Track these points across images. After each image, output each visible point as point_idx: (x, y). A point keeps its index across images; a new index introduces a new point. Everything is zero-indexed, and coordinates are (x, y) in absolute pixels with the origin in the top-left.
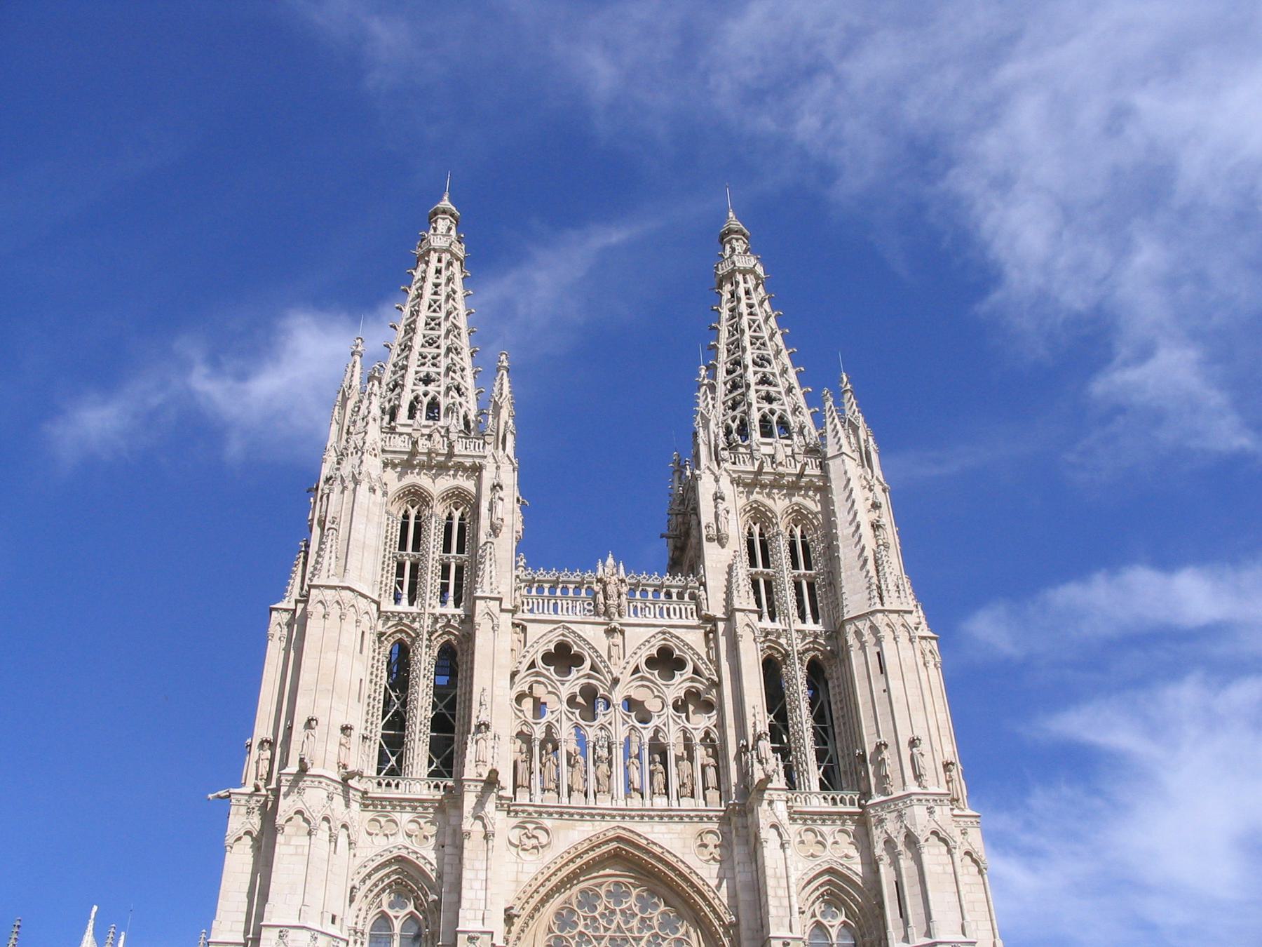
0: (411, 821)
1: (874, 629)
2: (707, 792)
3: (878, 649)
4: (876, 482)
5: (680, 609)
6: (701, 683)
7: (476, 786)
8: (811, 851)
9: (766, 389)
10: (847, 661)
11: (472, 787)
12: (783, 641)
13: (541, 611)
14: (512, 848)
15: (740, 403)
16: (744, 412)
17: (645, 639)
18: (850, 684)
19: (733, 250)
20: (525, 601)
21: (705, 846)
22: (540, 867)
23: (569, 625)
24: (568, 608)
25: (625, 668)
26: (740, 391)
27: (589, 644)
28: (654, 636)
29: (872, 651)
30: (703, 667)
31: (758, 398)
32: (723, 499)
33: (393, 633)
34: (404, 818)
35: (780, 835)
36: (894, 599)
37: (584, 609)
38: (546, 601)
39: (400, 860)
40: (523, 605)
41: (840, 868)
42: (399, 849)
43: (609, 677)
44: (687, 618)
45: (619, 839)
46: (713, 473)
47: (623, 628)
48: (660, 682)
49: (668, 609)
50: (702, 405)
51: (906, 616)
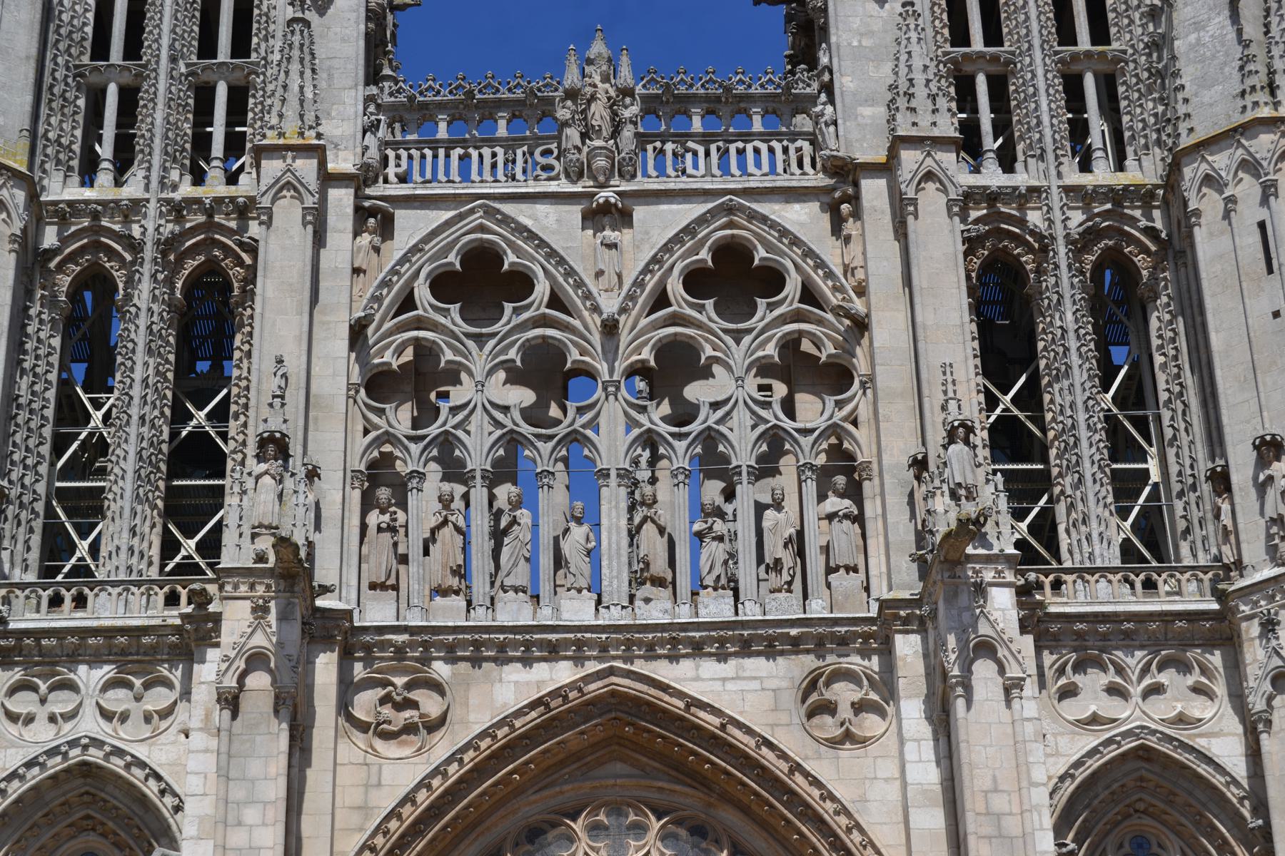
0: (110, 685)
1: (1250, 166)
2: (832, 577)
3: (1263, 214)
5: (771, 151)
6: (820, 322)
7: (252, 587)
8: (1093, 708)
10: (1189, 252)
11: (243, 589)
12: (1034, 218)
13: (428, 176)
14: (359, 737)
18: (1196, 310)
20: (391, 153)
21: (828, 708)
22: (420, 770)
24: (494, 166)
27: (542, 244)
28: (702, 220)
29: (1250, 212)
30: (825, 287)
33: (82, 250)
34: (90, 677)
35: (1002, 670)
38: (441, 152)
39: (86, 769)
40: (386, 166)
41: (1165, 748)
42: (85, 747)
43: (594, 321)
45: (616, 700)
47: (628, 202)
48: (719, 324)
49: (741, 152)
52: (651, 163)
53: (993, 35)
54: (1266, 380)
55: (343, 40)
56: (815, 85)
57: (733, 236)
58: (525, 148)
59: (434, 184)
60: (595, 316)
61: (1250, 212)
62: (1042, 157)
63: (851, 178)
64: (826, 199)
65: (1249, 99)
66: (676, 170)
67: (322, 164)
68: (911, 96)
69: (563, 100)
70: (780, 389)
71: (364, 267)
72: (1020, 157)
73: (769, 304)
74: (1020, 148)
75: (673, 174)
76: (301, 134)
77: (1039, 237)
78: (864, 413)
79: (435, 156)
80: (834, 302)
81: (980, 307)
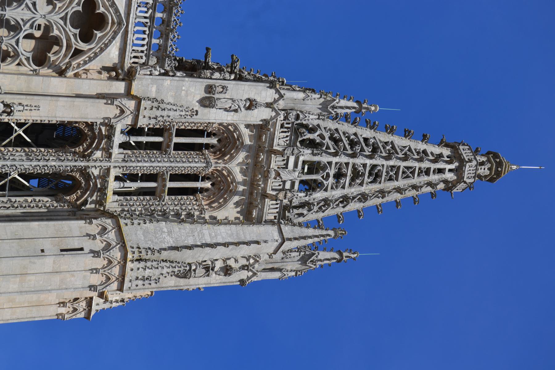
1: (108, 247)
3: (86, 250)
4: (250, 274)
5: (143, 46)
6: (65, 56)
9: (349, 174)
10: (74, 217)
12: (98, 154)
15: (337, 146)
16: (328, 148)
19: (482, 164)
26: (348, 147)
28: (117, 11)
29: (88, 245)
30: (80, 60)
31: (341, 164)
32: (249, 108)
36: (134, 274)
46: (276, 101)
48: (70, 11)
49: (144, 32)
50: (343, 103)
51: (115, 286)
53: (179, 147)
54: (15, 243)
56: (168, 69)
57: (108, 23)
61: (88, 245)
62: (124, 160)
63: (126, 78)
64: (118, 66)
65: (136, 250)
66: (140, 3)
68: (158, 109)
70: (38, 34)
72: (125, 152)
73: (76, 34)
74: (129, 152)
77: (90, 155)
78: (22, 69)
80: (73, 63)
81: (63, 126)
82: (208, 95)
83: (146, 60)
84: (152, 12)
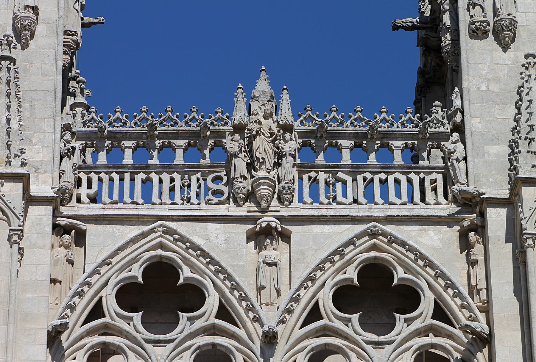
6: (450, 336)
13: (116, 197)
17: (332, 249)
23: (173, 225)
24: (172, 189)
25: (289, 311)
27: (213, 262)
37: (207, 189)
38: (127, 176)
43: (257, 331)
44: (423, 199)
49: (384, 182)
52: (306, 191)
55: (43, 74)
56: (448, 127)
57: (376, 258)
58: (199, 175)
59: (120, 205)
60: (257, 325)
63: (478, 209)
66: (328, 198)
67: (26, 189)
69: (232, 134)
71: (60, 279)
73: (406, 320)
75: (325, 201)
76: (9, 163)
79: (122, 180)
80: (464, 321)
82: (491, 34)
83: (436, 172)
84: (342, 172)
